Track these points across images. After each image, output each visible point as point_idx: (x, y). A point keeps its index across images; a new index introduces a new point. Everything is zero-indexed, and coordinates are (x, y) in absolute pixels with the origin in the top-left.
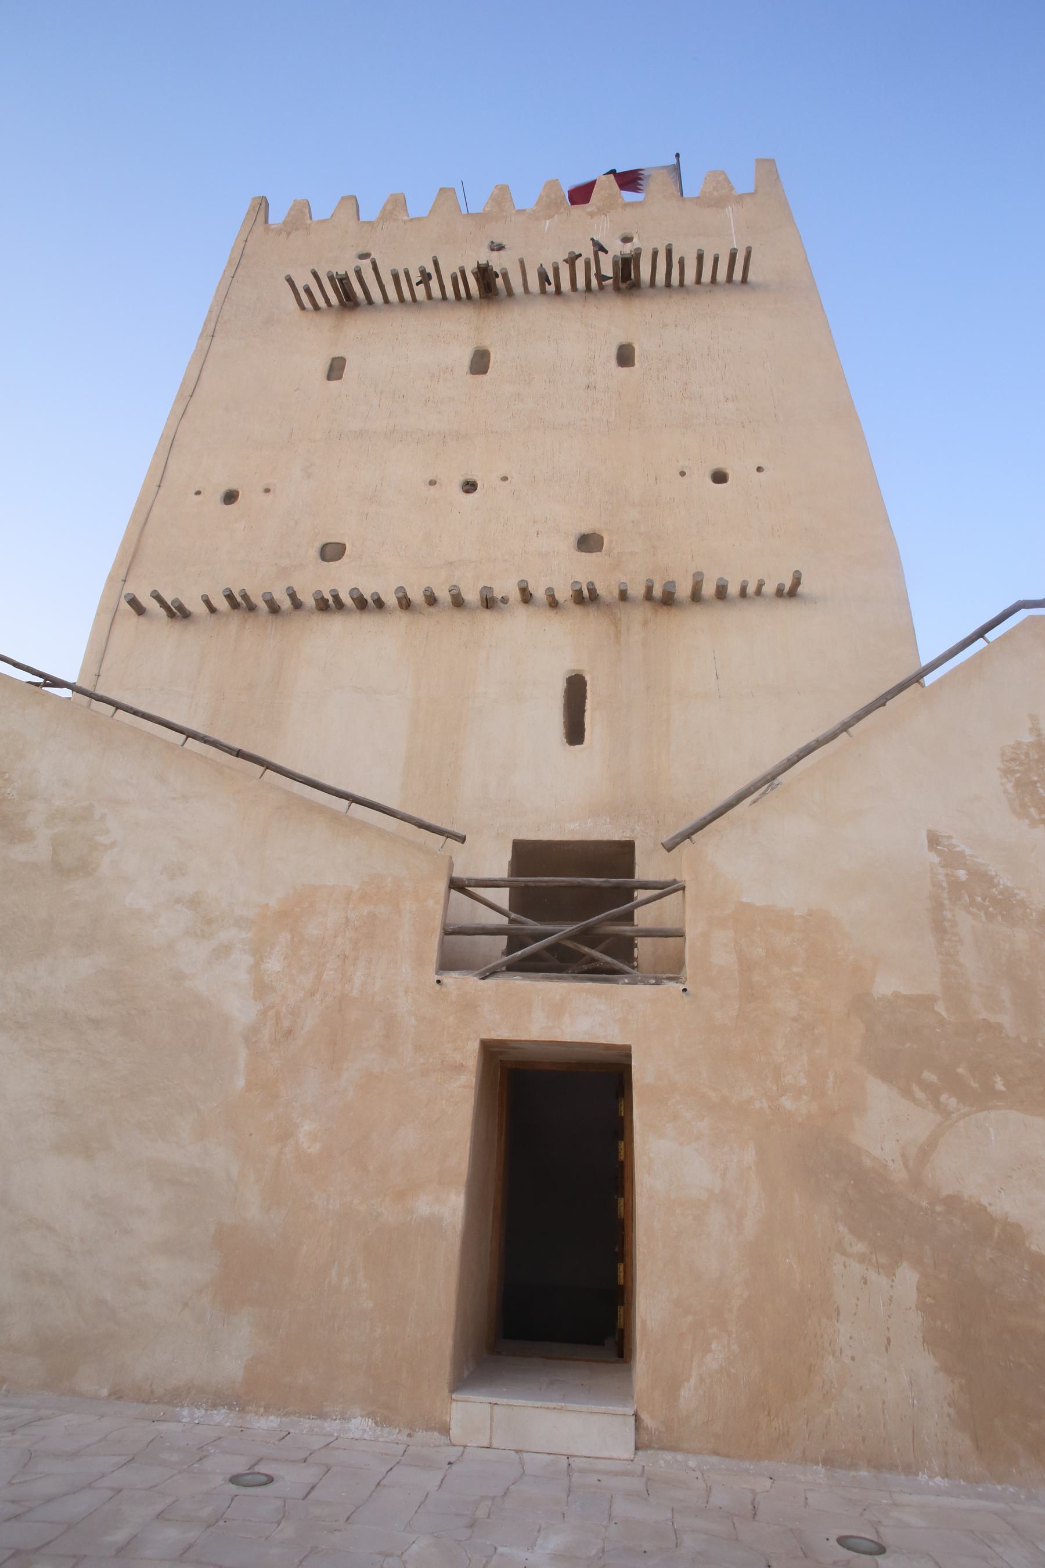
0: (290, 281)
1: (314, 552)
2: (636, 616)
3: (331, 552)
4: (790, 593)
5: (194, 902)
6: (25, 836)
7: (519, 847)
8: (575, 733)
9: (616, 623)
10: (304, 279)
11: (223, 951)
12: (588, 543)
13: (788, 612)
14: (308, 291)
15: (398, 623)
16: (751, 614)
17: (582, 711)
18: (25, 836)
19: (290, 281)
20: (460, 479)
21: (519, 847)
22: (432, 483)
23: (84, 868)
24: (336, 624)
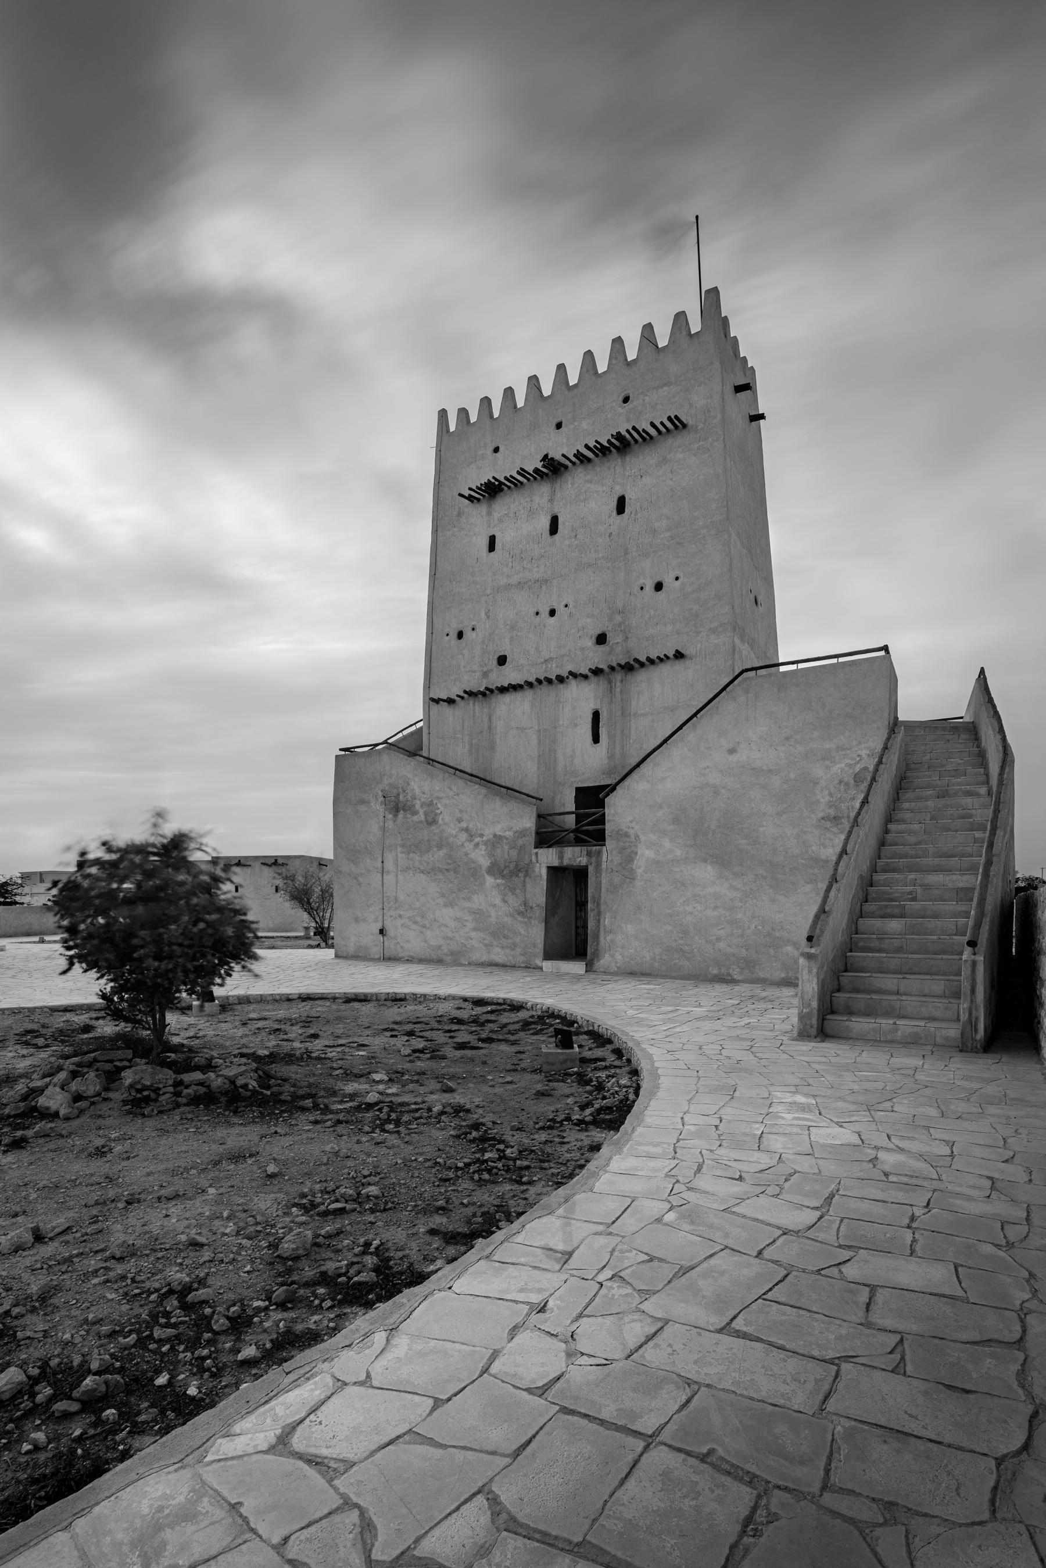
0: (461, 495)
1: (495, 662)
2: (618, 676)
3: (502, 660)
4: (679, 655)
5: (467, 830)
6: (416, 813)
7: (579, 791)
8: (596, 739)
9: (610, 682)
10: (467, 493)
11: (477, 845)
12: (601, 639)
13: (679, 665)
14: (470, 495)
15: (529, 693)
16: (664, 669)
17: (598, 728)
18: (416, 813)
19: (461, 495)
20: (548, 610)
21: (579, 791)
22: (537, 614)
23: (434, 822)
24: (507, 698)
